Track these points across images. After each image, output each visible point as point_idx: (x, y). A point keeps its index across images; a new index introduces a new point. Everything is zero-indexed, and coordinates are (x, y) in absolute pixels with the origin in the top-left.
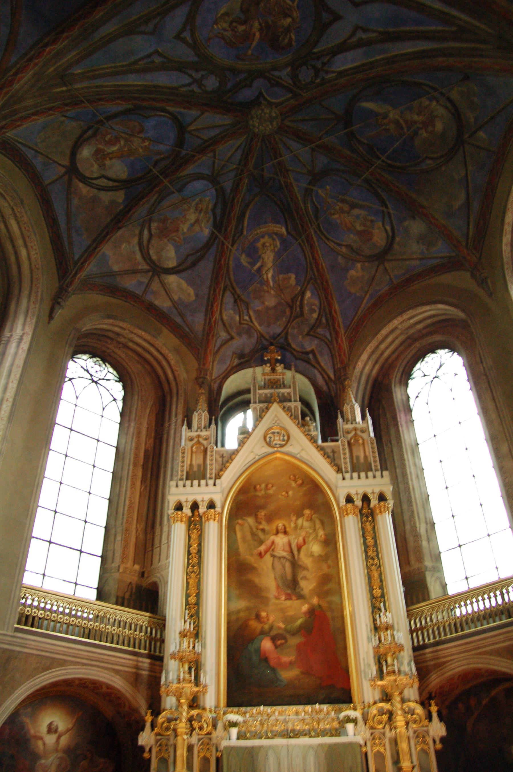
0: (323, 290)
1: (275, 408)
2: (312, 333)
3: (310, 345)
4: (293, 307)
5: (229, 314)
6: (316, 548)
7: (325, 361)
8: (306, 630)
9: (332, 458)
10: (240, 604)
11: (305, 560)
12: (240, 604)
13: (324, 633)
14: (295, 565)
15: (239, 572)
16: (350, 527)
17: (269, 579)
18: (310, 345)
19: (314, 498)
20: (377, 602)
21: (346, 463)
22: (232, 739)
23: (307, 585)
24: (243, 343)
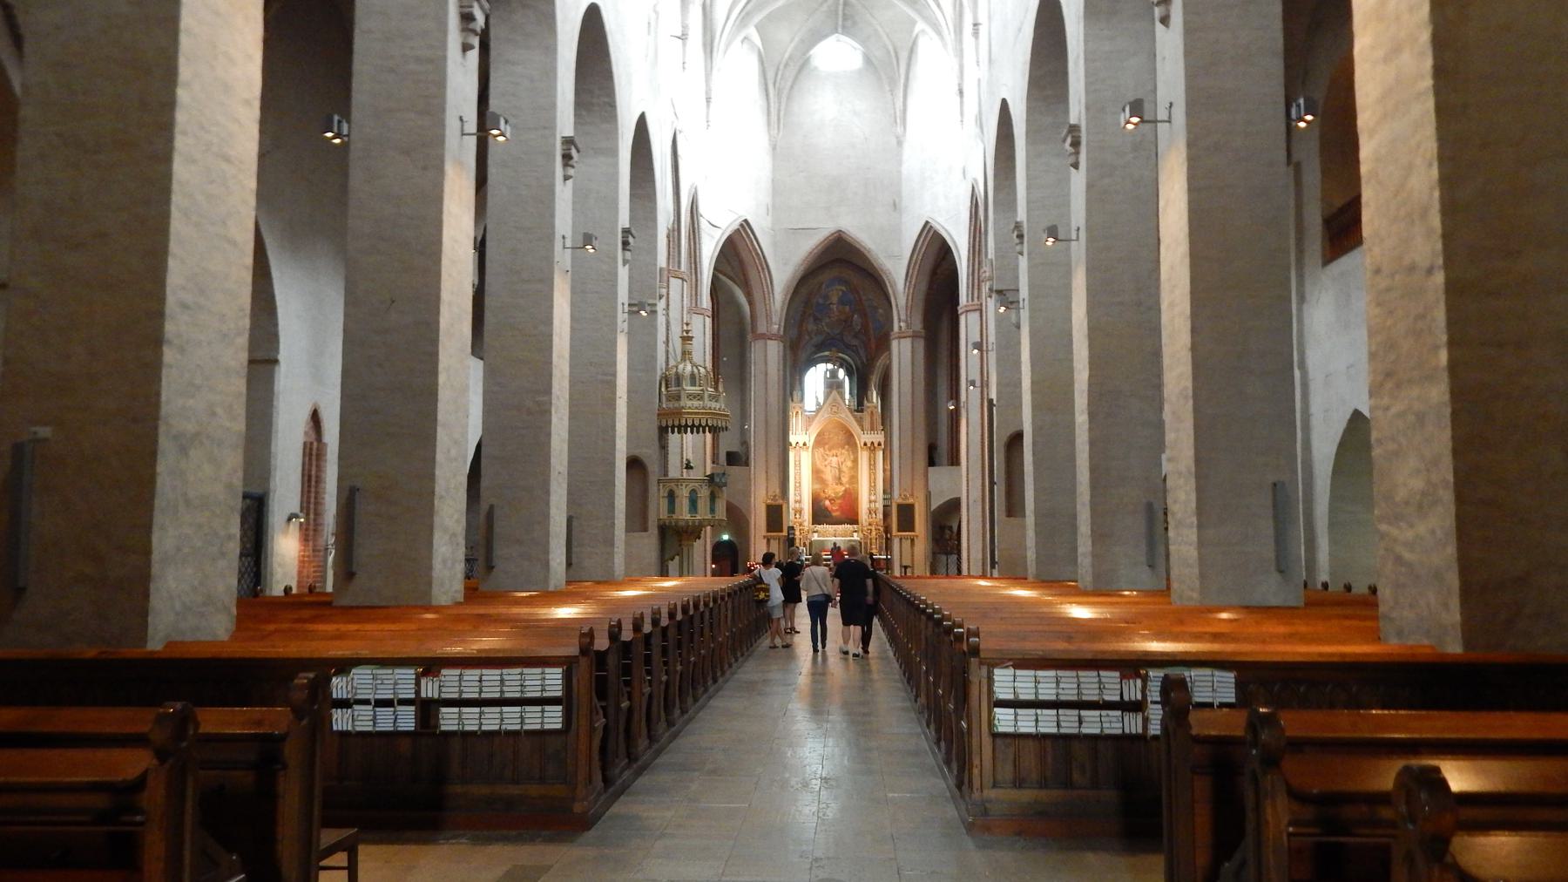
0: (864, 315)
1: (835, 393)
2: (855, 336)
3: (855, 342)
4: (847, 322)
5: (811, 326)
6: (849, 464)
7: (862, 353)
8: (843, 497)
9: (860, 422)
10: (817, 486)
11: (844, 468)
12: (817, 486)
13: (850, 500)
14: (840, 471)
15: (817, 474)
16: (864, 457)
17: (829, 475)
18: (855, 342)
19: (850, 440)
20: (872, 488)
21: (867, 424)
22: (815, 537)
23: (844, 480)
24: (817, 339)
